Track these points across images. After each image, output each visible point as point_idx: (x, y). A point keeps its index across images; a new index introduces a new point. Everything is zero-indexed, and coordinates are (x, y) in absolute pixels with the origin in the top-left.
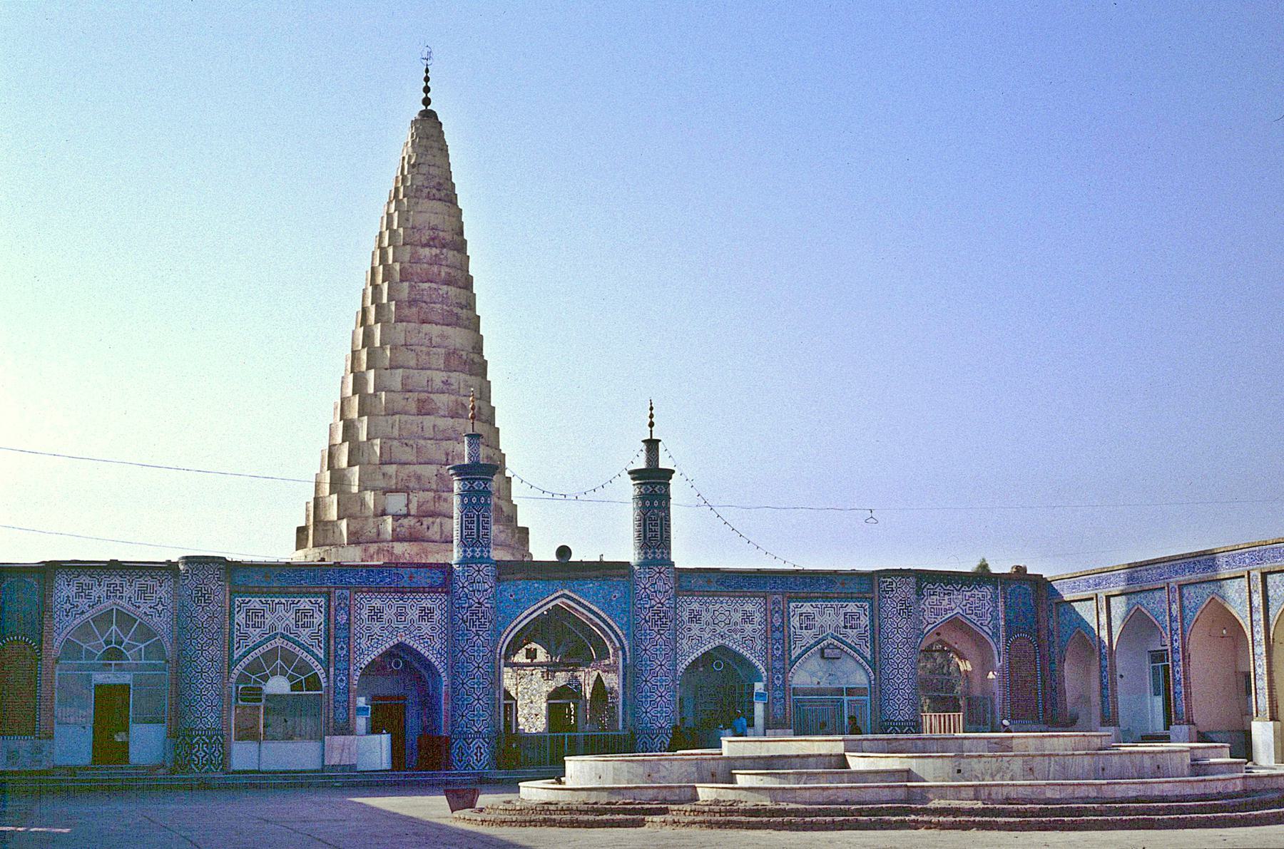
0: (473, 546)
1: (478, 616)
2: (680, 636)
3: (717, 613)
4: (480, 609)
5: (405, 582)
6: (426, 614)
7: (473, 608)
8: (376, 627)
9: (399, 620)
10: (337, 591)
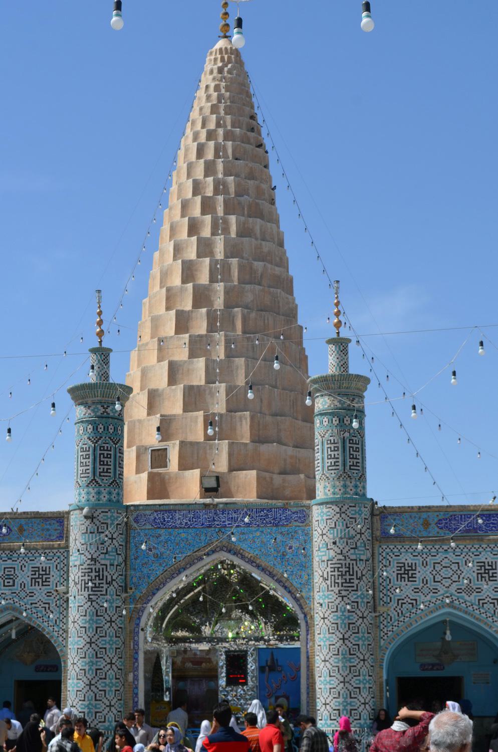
0: (87, 486)
2: (385, 599)
3: (438, 567)
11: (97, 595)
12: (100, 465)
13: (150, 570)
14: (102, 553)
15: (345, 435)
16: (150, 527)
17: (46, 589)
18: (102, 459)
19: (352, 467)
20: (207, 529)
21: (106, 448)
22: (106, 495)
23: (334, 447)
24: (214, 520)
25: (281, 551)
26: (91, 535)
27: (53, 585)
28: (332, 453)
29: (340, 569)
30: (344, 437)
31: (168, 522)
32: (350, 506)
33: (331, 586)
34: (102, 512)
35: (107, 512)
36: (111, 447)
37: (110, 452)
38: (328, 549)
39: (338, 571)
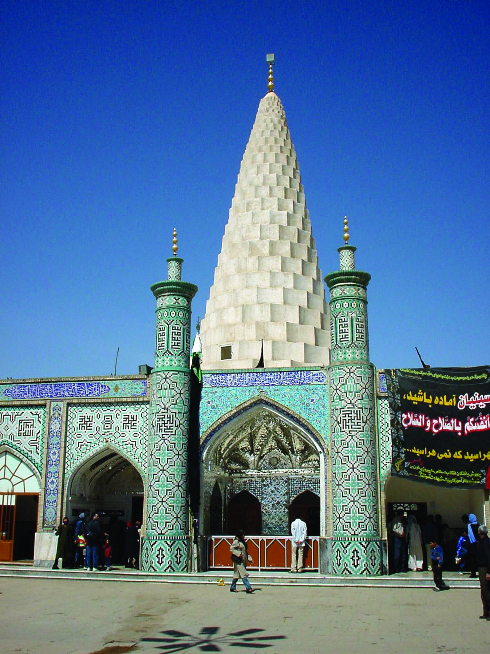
1: (164, 421)
2: (384, 439)
4: (166, 414)
5: (112, 393)
6: (130, 422)
7: (160, 413)
8: (85, 435)
9: (105, 428)
10: (52, 403)
11: (168, 435)
12: (172, 340)
13: (209, 417)
14: (172, 404)
15: (352, 315)
16: (209, 386)
17: (134, 431)
18: (174, 336)
19: (358, 339)
20: (250, 387)
21: (177, 328)
22: (176, 362)
23: (345, 324)
24: (256, 381)
25: (306, 403)
26: (164, 390)
27: (138, 428)
28: (343, 329)
29: (350, 415)
30: (352, 317)
31: (222, 382)
32: (357, 368)
33: (343, 428)
34: (173, 374)
35: (177, 374)
36: (180, 328)
37: (179, 331)
38: (340, 400)
39: (349, 416)
